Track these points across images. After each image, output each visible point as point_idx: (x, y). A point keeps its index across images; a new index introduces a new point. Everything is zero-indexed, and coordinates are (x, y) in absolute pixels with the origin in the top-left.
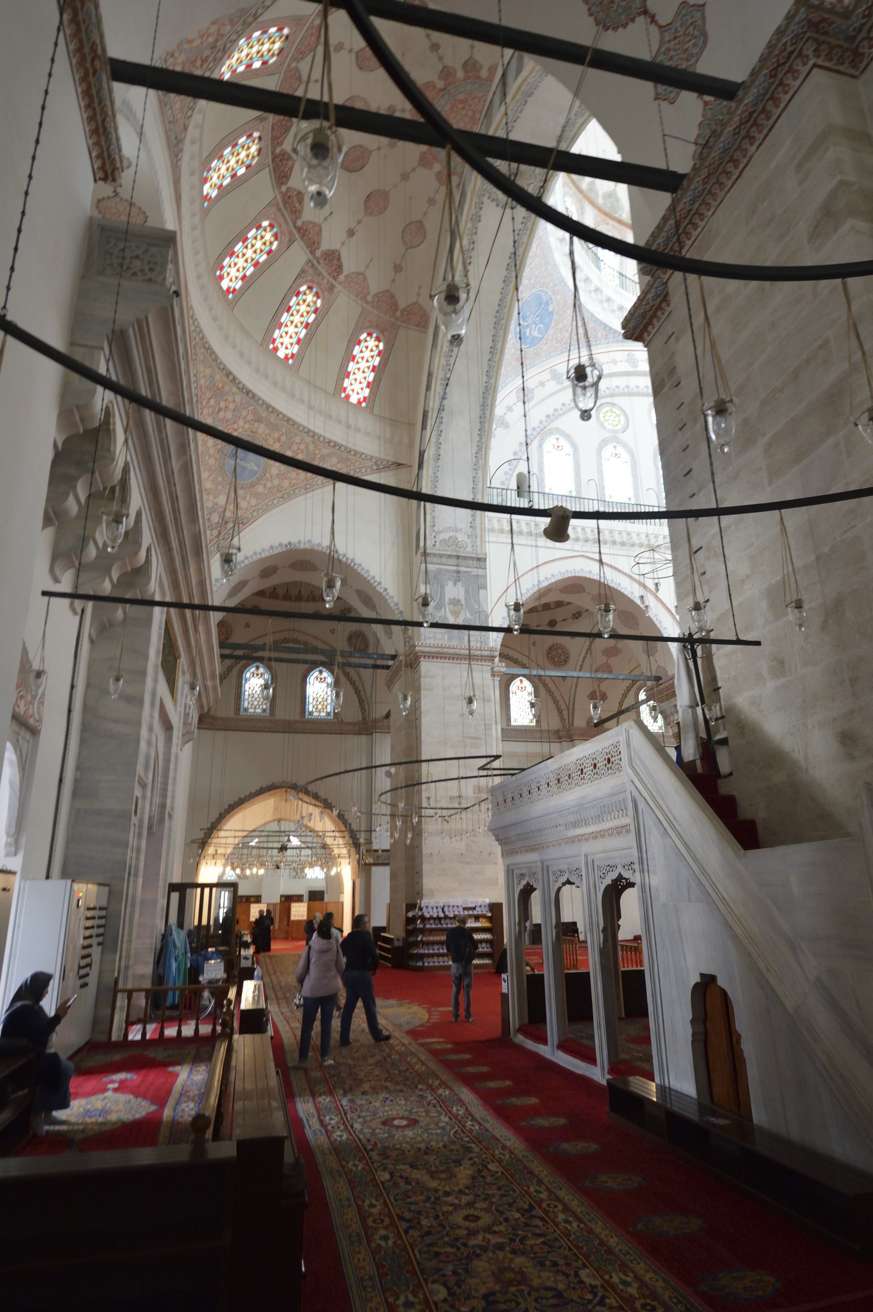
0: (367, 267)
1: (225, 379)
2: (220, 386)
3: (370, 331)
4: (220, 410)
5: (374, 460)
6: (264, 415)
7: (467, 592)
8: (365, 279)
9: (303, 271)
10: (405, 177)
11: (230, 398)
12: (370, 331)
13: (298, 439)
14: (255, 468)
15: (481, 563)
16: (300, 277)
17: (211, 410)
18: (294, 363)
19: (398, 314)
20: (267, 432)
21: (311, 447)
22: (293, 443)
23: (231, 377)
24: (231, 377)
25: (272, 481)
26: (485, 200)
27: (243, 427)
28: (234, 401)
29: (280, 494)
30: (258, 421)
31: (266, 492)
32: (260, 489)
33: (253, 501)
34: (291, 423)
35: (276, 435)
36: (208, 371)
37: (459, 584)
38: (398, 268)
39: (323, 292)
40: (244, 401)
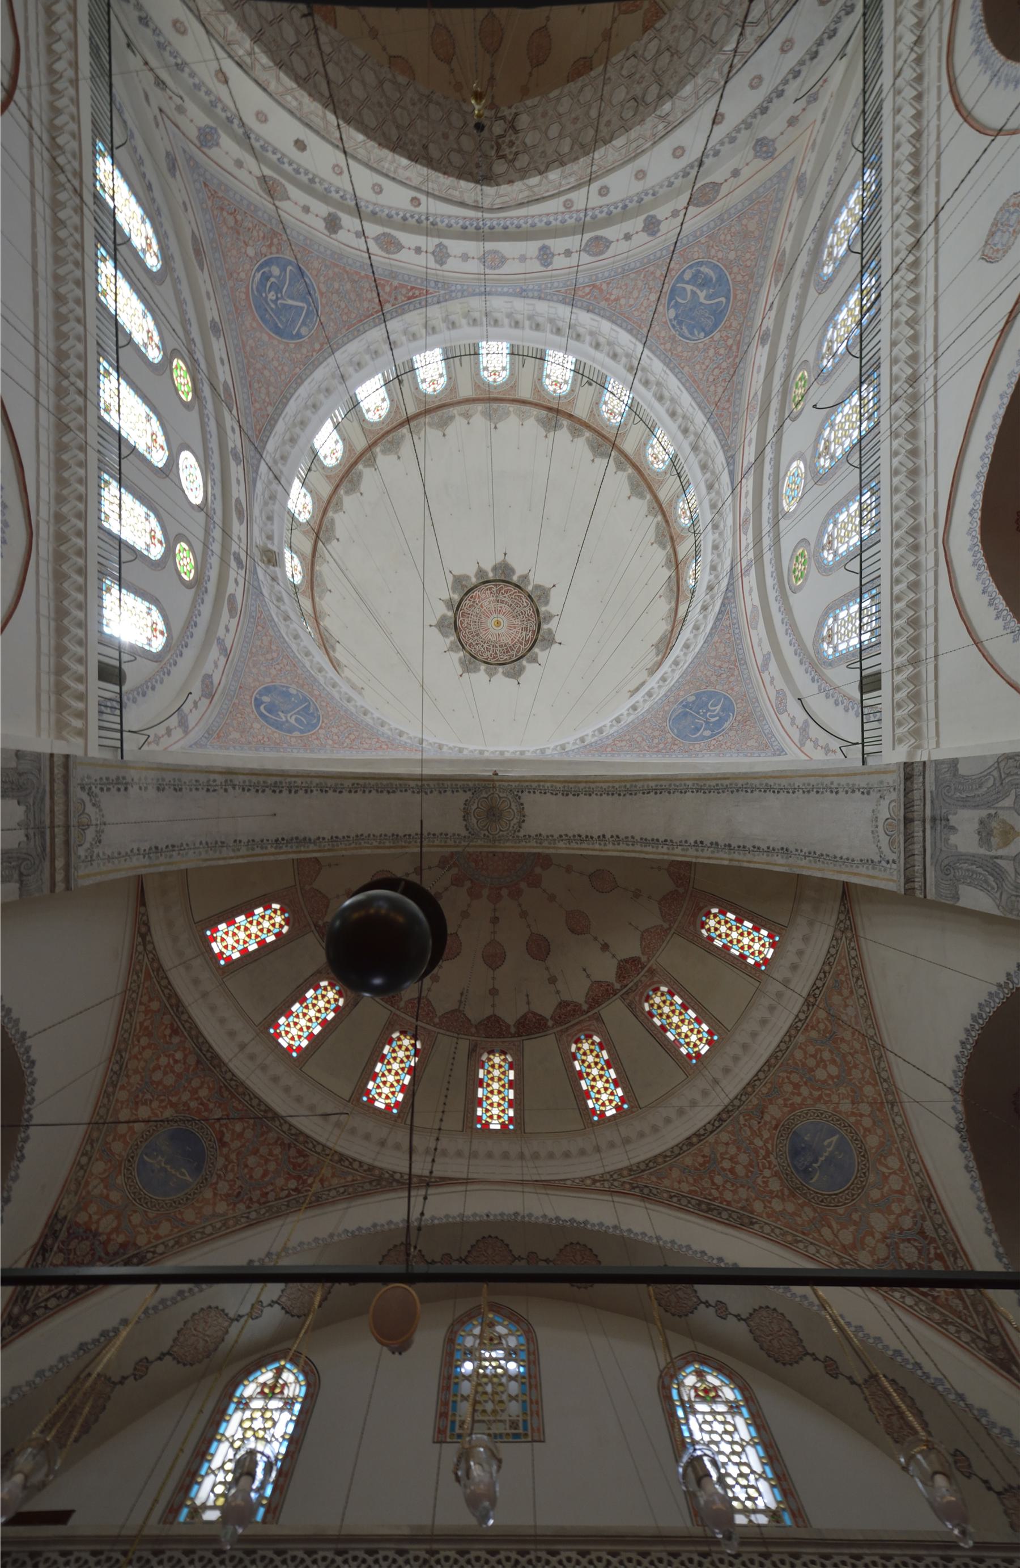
0: (636, 928)
1: (693, 1150)
2: (701, 1160)
3: (699, 923)
4: (732, 1171)
5: (838, 934)
6: (755, 1102)
7: (965, 803)
8: (647, 930)
9: (629, 1006)
10: (552, 898)
11: (721, 1149)
12: (699, 923)
13: (799, 1055)
14: (835, 1138)
15: (918, 770)
16: (634, 1009)
17: (728, 1186)
18: (719, 1034)
19: (681, 890)
20: (780, 1101)
21: (814, 1034)
22: (804, 1064)
23: (695, 1140)
24: (695, 1140)
25: (861, 1115)
26: (521, 834)
27: (766, 1142)
28: (727, 1144)
29: (887, 1108)
30: (762, 1113)
31: (879, 1132)
32: (872, 1141)
33: (893, 1162)
34: (773, 1061)
35: (789, 1088)
36: (675, 1173)
37: (953, 820)
38: (637, 894)
39: (654, 983)
40: (730, 1128)
